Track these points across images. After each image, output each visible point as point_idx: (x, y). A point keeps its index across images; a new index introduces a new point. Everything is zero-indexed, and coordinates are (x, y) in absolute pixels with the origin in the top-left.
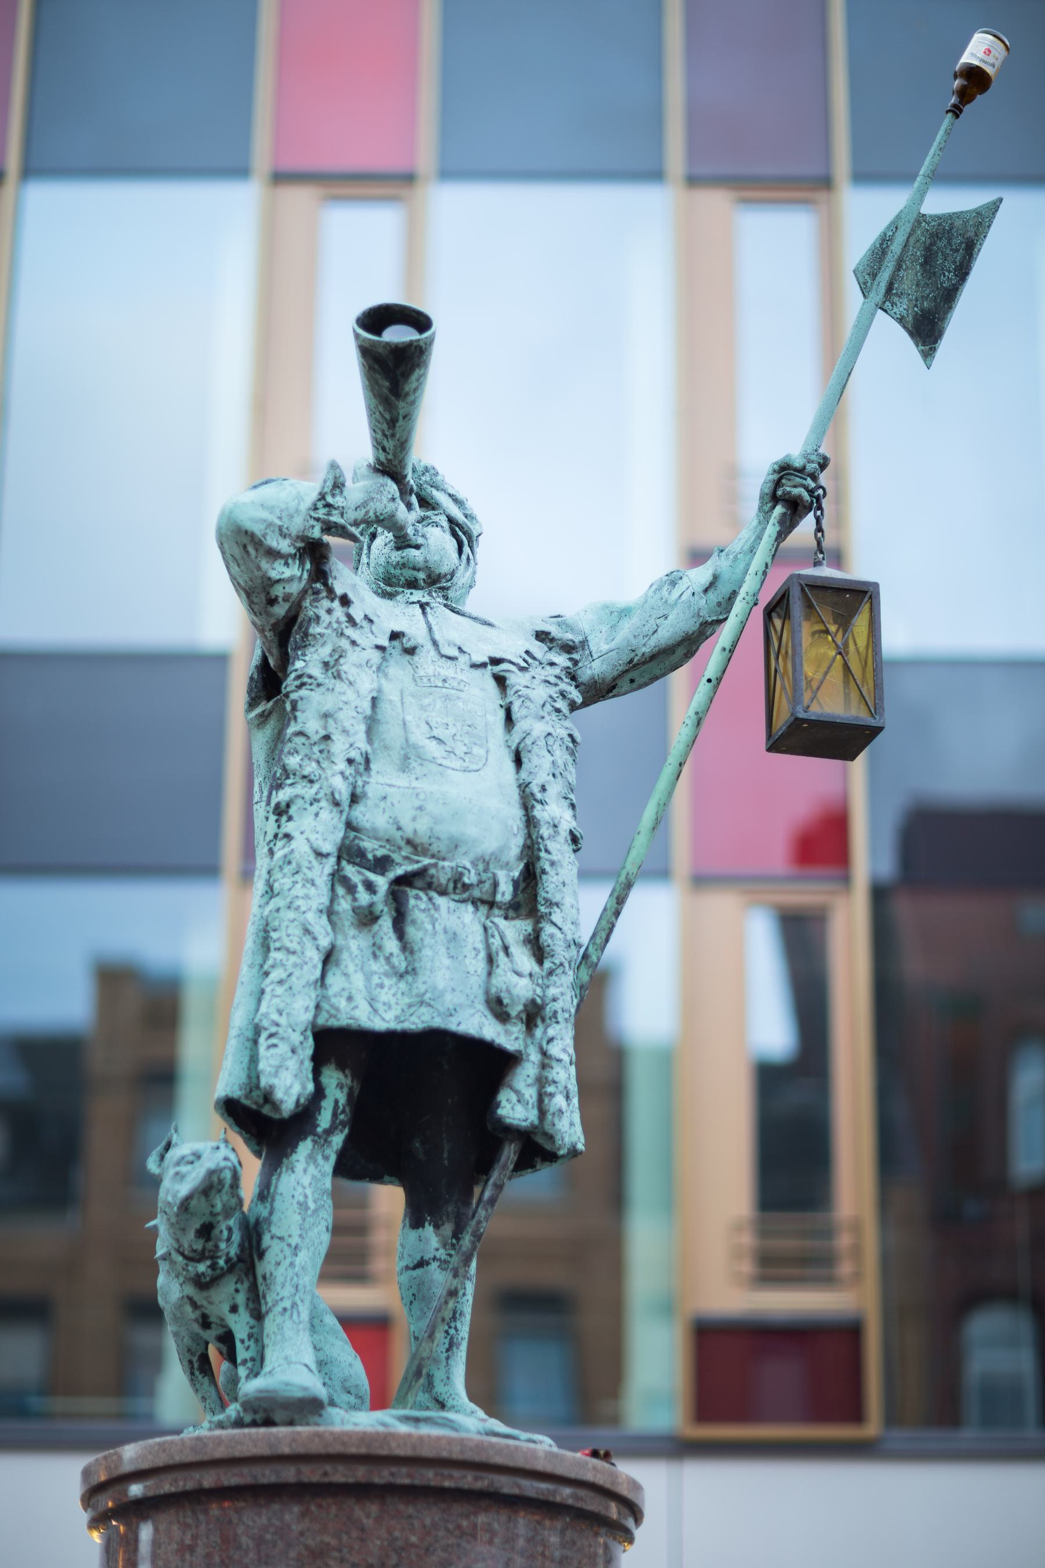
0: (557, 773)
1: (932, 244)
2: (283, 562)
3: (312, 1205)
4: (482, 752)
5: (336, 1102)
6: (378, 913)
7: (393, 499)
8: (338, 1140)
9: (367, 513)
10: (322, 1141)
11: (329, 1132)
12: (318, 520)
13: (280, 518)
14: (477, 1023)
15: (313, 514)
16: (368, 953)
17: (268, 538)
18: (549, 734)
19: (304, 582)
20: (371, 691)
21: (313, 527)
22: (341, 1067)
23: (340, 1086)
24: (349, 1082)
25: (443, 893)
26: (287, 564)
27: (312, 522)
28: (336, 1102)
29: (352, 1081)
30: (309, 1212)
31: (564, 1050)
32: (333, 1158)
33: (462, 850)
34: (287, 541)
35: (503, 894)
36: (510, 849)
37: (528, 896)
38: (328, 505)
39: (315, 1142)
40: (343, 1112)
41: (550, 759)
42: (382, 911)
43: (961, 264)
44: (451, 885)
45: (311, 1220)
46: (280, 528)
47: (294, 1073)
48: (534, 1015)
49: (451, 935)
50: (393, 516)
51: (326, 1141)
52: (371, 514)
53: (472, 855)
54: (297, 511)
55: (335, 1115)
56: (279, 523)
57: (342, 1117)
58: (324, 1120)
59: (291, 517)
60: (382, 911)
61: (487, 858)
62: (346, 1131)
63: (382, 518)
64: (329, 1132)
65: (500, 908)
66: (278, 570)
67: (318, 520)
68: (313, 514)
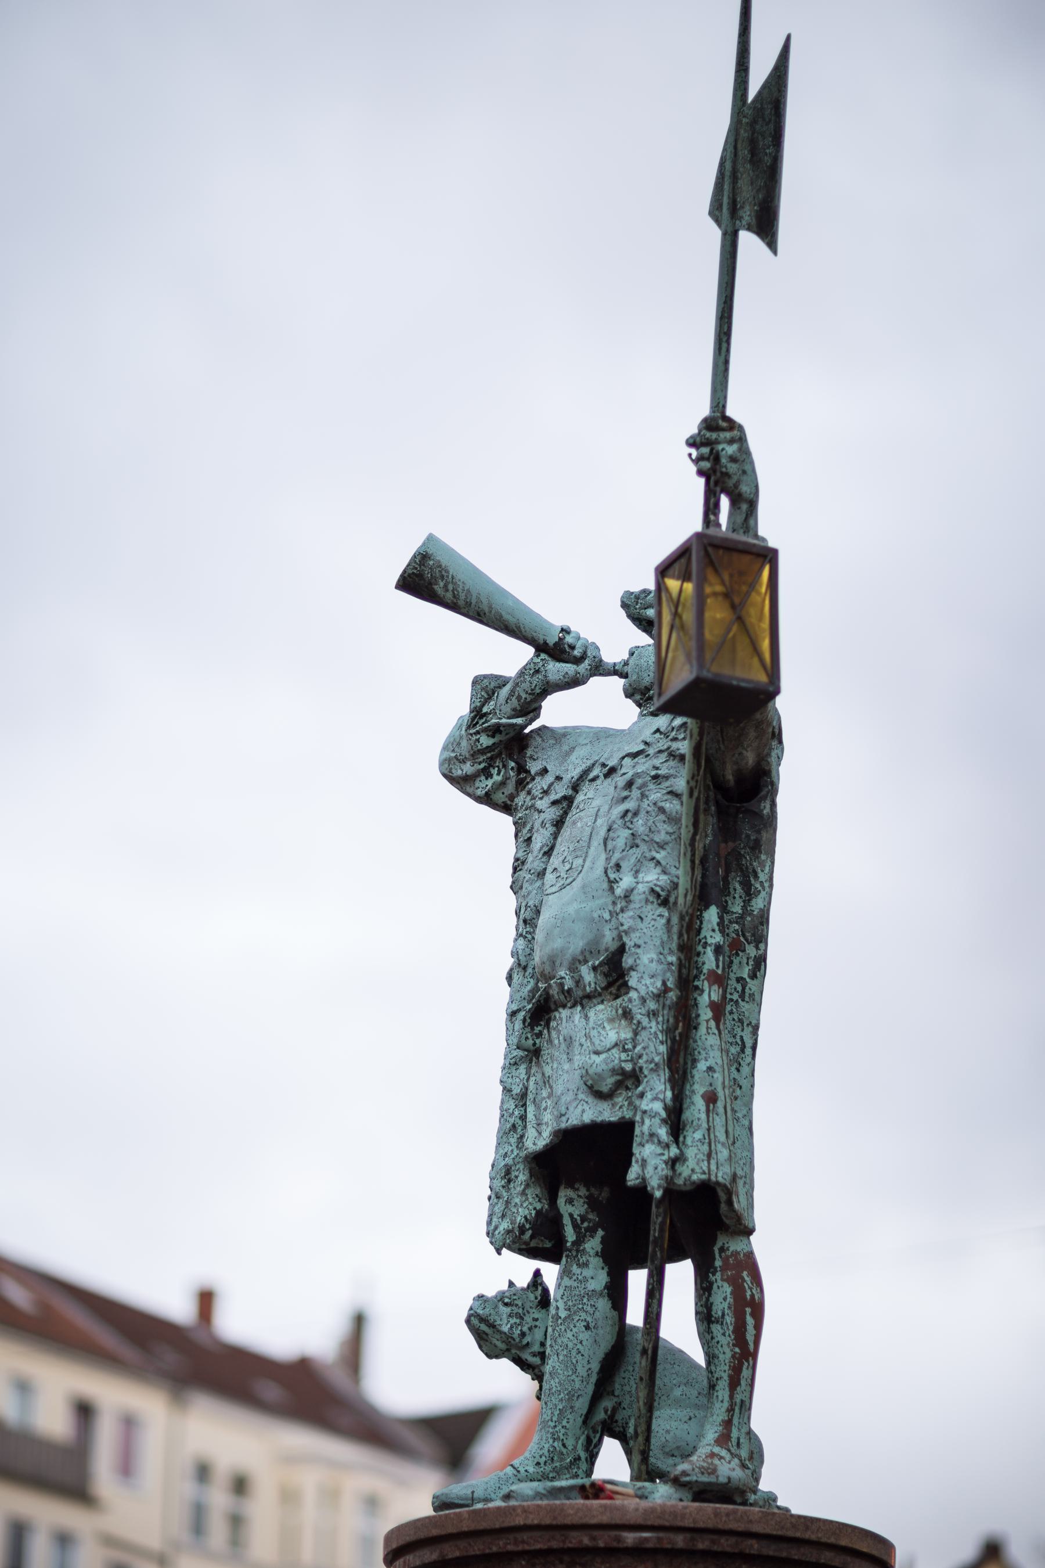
0: (638, 841)
1: (753, 133)
2: (483, 778)
3: (563, 1314)
4: (580, 861)
5: (571, 1215)
6: (532, 1048)
7: (537, 671)
8: (593, 1244)
9: (519, 698)
10: (574, 1253)
11: (578, 1243)
12: (478, 733)
13: (453, 751)
14: (588, 1112)
15: (472, 731)
16: (541, 1083)
17: (454, 771)
18: (627, 811)
19: (514, 780)
20: (541, 848)
21: (478, 740)
22: (571, 1185)
23: (570, 1201)
24: (583, 1191)
25: (564, 1006)
26: (489, 776)
27: (475, 738)
28: (571, 1215)
29: (588, 1190)
30: (560, 1321)
31: (656, 1098)
32: (596, 1262)
33: (558, 963)
34: (468, 763)
35: (590, 984)
36: (604, 936)
37: (615, 974)
38: (486, 714)
39: (567, 1256)
40: (583, 1219)
41: (628, 832)
42: (534, 1044)
43: (775, 131)
44: (562, 997)
45: (563, 1328)
46: (456, 757)
47: (500, 1215)
48: (629, 1079)
49: (568, 1039)
50: (548, 683)
51: (578, 1251)
52: (524, 696)
53: (566, 963)
54: (461, 737)
55: (575, 1226)
56: (453, 755)
57: (585, 1224)
58: (570, 1235)
59: (459, 744)
60: (534, 1044)
61: (581, 958)
62: (600, 1233)
63: (538, 691)
64: (578, 1243)
65: (595, 997)
66: (484, 785)
67: (478, 733)
68: (472, 731)
